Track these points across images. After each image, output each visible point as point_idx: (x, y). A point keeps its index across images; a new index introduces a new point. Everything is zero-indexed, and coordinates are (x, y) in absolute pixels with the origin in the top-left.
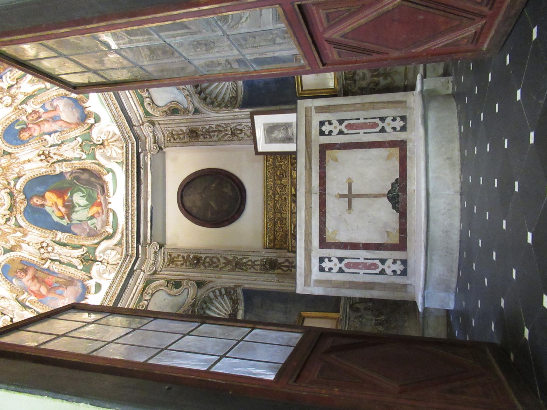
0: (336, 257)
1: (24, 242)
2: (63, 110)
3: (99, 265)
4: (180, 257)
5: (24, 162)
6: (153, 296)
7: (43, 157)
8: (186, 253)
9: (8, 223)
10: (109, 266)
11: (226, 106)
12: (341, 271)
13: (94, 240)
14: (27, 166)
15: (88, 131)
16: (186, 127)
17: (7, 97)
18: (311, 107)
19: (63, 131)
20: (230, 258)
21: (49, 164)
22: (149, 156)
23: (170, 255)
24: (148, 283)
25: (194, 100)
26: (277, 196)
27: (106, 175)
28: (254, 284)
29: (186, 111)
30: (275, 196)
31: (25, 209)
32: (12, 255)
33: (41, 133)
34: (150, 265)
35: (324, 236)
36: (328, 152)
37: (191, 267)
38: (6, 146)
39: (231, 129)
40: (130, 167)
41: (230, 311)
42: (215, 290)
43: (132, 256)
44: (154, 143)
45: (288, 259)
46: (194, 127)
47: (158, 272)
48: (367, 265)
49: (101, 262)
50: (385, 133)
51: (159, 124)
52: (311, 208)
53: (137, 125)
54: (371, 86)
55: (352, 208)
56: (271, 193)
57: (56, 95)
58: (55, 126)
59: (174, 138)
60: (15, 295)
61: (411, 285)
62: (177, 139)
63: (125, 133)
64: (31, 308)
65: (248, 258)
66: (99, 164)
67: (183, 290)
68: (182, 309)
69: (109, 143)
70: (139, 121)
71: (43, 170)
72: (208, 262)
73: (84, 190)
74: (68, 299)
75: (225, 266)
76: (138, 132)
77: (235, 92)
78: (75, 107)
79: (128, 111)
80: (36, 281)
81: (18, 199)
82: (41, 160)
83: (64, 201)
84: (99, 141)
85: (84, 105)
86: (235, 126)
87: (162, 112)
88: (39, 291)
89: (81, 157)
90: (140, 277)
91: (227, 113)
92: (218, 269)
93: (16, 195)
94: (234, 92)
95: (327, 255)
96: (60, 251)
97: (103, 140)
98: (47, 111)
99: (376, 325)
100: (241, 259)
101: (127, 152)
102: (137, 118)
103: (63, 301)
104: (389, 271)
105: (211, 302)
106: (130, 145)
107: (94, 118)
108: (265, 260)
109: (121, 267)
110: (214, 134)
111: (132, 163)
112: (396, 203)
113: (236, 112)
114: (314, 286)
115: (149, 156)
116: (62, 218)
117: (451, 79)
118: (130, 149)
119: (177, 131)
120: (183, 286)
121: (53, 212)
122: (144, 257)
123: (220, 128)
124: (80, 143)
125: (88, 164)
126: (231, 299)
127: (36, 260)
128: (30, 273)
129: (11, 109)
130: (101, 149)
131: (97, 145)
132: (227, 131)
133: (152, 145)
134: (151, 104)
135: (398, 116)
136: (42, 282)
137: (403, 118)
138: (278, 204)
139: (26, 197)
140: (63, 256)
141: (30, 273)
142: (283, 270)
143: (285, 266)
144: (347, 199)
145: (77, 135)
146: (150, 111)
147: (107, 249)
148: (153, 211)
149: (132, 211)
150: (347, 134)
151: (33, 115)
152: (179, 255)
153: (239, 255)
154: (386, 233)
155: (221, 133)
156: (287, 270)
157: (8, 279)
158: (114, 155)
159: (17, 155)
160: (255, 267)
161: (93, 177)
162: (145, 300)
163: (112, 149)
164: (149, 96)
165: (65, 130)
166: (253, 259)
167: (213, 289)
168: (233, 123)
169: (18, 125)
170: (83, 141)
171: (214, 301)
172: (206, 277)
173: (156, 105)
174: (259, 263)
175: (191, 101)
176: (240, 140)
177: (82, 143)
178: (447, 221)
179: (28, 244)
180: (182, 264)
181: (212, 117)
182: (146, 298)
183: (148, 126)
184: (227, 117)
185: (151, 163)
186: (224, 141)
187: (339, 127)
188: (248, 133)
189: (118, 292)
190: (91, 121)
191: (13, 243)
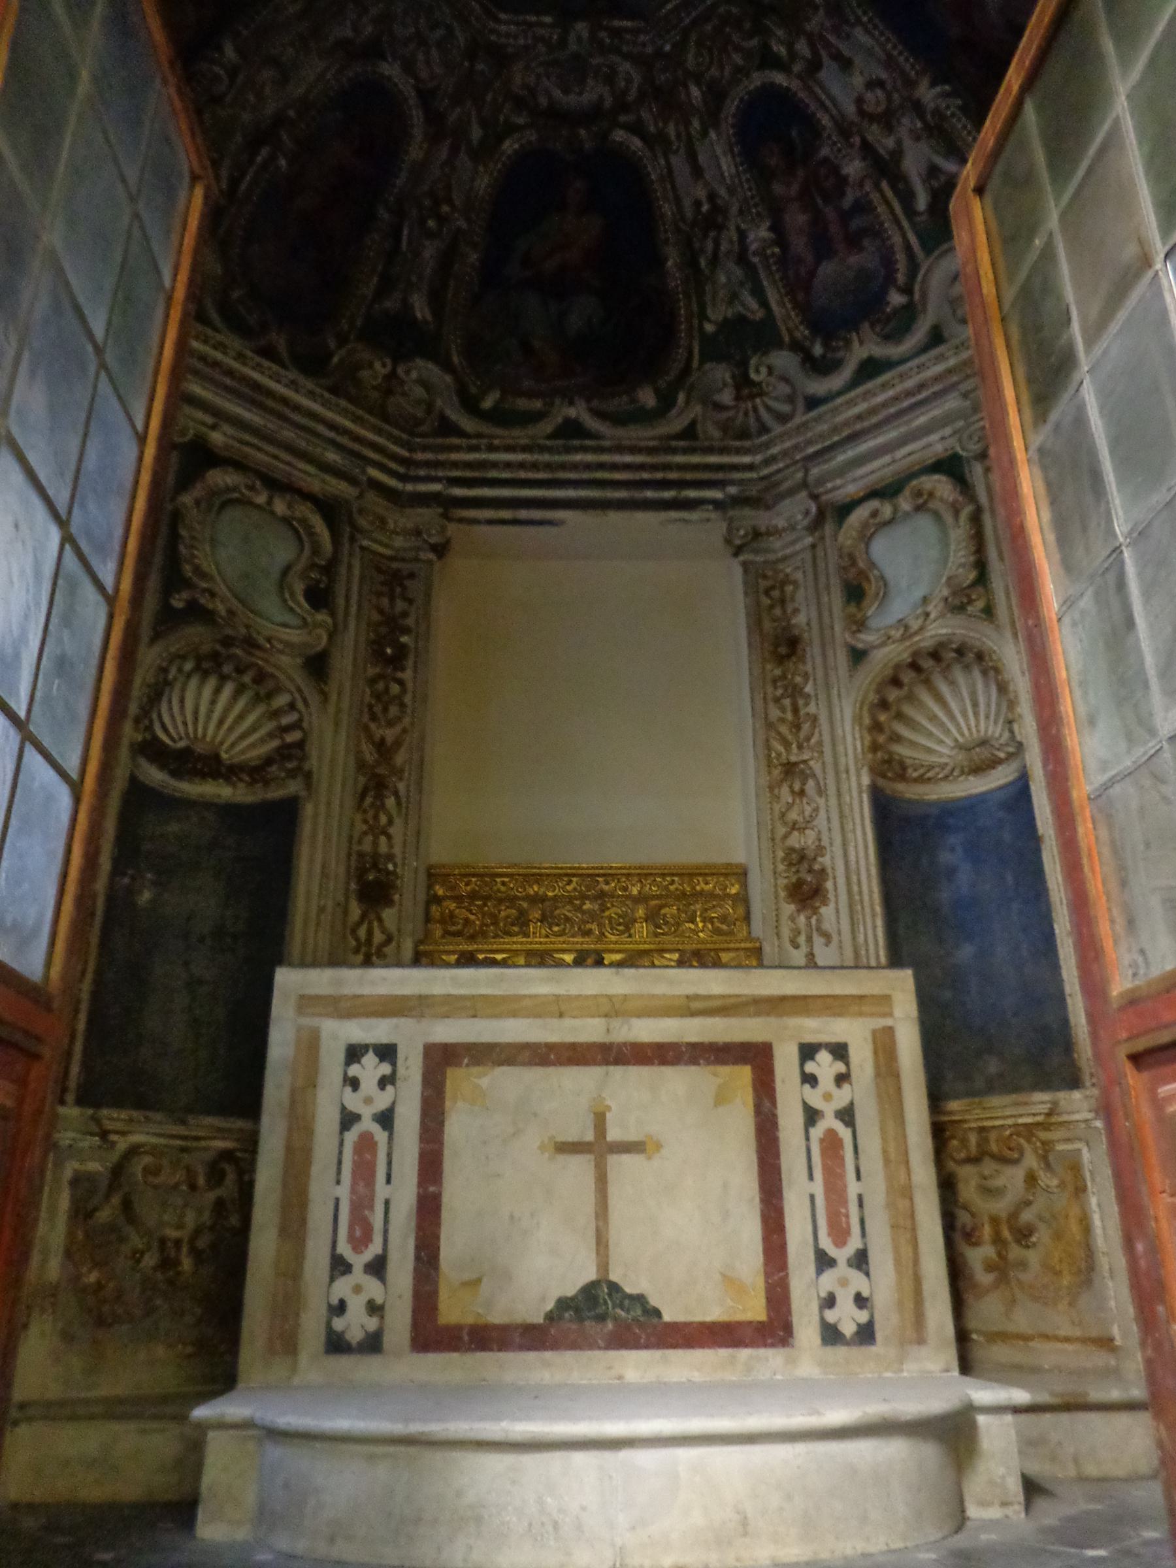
0: (394, 1103)
1: (454, 150)
5: (692, 156)
11: (875, 747)
12: (348, 1119)
15: (787, 339)
16: (808, 624)
18: (890, 1014)
20: (399, 759)
23: (412, 576)
25: (893, 646)
26: (597, 907)
28: (314, 835)
30: (595, 898)
35: (466, 1061)
36: (745, 1073)
39: (805, 762)
42: (300, 712)
45: (394, 944)
48: (367, 1212)
50: (812, 1268)
51: (813, 546)
52: (561, 1015)
54: (963, 1218)
55: (562, 1158)
56: (606, 888)
58: (799, 244)
59: (773, 588)
61: (294, 1369)
62: (771, 598)
68: (240, 605)
71: (668, 209)
72: (387, 690)
77: (922, 775)
82: (698, 204)
84: (757, 371)
86: (814, 776)
91: (855, 749)
94: (921, 771)
95: (401, 1071)
97: (760, 384)
98: (845, 217)
99: (163, 1242)
100: (396, 794)
104: (342, 1288)
105: (257, 699)
106: (746, 459)
108: (390, 867)
110: (789, 708)
112: (577, 1310)
113: (858, 776)
114: (299, 1029)
117: (1016, 1512)
119: (793, 599)
120: (313, 611)
123: (806, 727)
126: (268, 761)
132: (800, 747)
135: (872, 1316)
137: (866, 1334)
138: (569, 911)
142: (359, 924)
143: (370, 933)
144: (589, 1137)
150: (808, 1139)
152: (410, 601)
153: (408, 786)
154: (474, 1276)
156: (357, 939)
160: (370, 838)
166: (396, 830)
167: (300, 704)
173: (872, 535)
174: (383, 848)
175: (889, 638)
176: (771, 788)
178: (514, 1519)
180: (381, 611)
186: (767, 741)
187: (828, 1110)
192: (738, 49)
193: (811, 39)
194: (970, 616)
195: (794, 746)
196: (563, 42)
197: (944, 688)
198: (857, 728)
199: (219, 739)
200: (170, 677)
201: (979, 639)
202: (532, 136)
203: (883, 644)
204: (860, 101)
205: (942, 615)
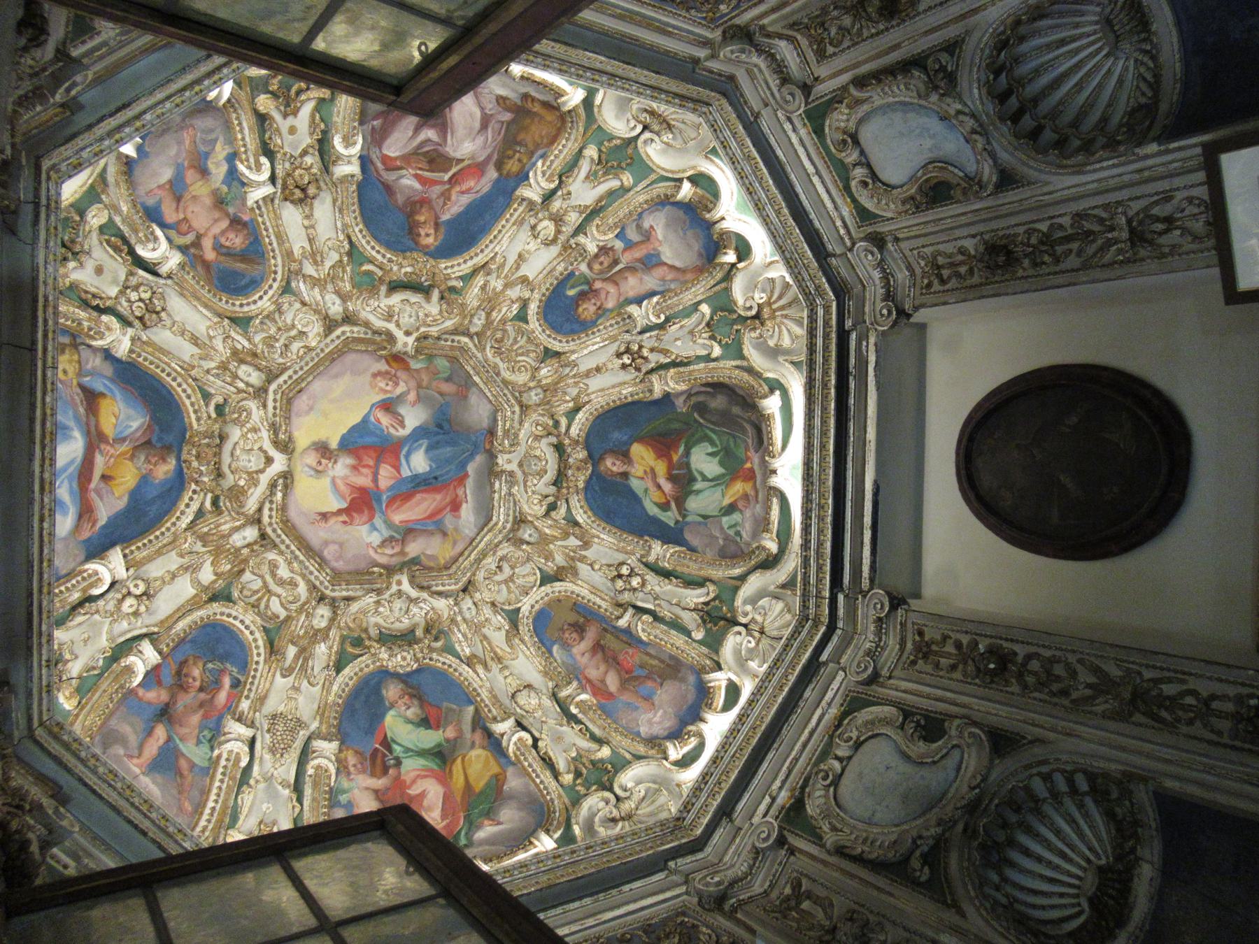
1: (582, 559)
2: (665, 237)
3: (740, 633)
4: (950, 642)
5: (588, 374)
6: (862, 750)
7: (626, 360)
8: (967, 632)
9: (553, 514)
10: (765, 642)
11: (1112, 144)
13: (733, 567)
14: (595, 383)
15: (723, 285)
16: (974, 236)
17: (546, 223)
20: (1115, 672)
21: (641, 375)
22: (872, 340)
23: (921, 633)
24: (853, 705)
27: (765, 397)
29: (973, 184)
31: (588, 482)
32: (557, 589)
33: (622, 299)
34: (861, 653)
37: (977, 681)
38: (549, 336)
39: (1129, 222)
40: (818, 374)
41: (1107, 858)
42: (1053, 771)
43: (816, 623)
44: (884, 300)
46: (1001, 233)
49: (745, 626)
53: (838, 252)
57: (646, 202)
59: (940, 277)
60: (550, 684)
62: (950, 278)
63: (807, 277)
64: (579, 722)
65: (1183, 682)
66: (750, 370)
67: (945, 751)
68: (935, 810)
69: (775, 311)
70: (842, 238)
72: (1035, 674)
73: (714, 436)
74: (660, 713)
75: (1093, 698)
76: (844, 272)
77: (1150, 85)
78: (691, 227)
79: (812, 216)
80: (599, 655)
81: (571, 460)
82: (624, 366)
83: (671, 466)
84: (751, 308)
85: (708, 216)
86: (1146, 209)
87: (904, 203)
88: (603, 681)
90: (835, 685)
91: (1114, 166)
92: (1066, 702)
93: (569, 450)
94: (1143, 86)
96: (657, 589)
98: (630, 246)
100: (1156, 681)
101: (812, 333)
103: (650, 715)
105: (1038, 812)
106: (820, 312)
107: (737, 250)
111: (826, 360)
113: (1147, 157)
115: (872, 340)
116: (665, 507)
118: (820, 322)
121: (646, 490)
122: (850, 629)
123: (1087, 225)
124: (708, 317)
125: (727, 370)
126: (1110, 815)
127: (604, 605)
128: (591, 634)
129: (555, 250)
130: (754, 329)
132: (1112, 229)
133: (879, 305)
134: (870, 181)
136: (612, 660)
139: (590, 456)
140: (663, 603)
141: (591, 634)
145: (699, 298)
146: (869, 205)
147: (761, 594)
148: (880, 498)
149: (822, 495)
151: (602, 259)
153: (1147, 666)
155: (1093, 241)
157: (543, 644)
158: (786, 342)
159: (573, 357)
160: (1213, 720)
161: (737, 404)
162: (837, 758)
164: (864, 160)
165: (673, 286)
166: (1205, 688)
167: (1044, 769)
168: (1137, 198)
169: (573, 287)
170: (713, 313)
171: (1048, 809)
172: (1025, 722)
173: (884, 184)
174: (1229, 707)
176: (1164, 256)
177: (712, 318)
179: (591, 565)
180: (953, 668)
181: (1057, 191)
182: (840, 753)
184: (1112, 182)
185: (877, 357)
186: (1103, 266)
188: (1199, 226)
189: (768, 720)
190: (730, 257)
191: (560, 560)
192: (516, 341)
193: (507, 286)
194: (958, 65)
195: (1110, 236)
196: (511, 474)
197: (1044, 80)
198: (1088, 168)
199: (1083, 864)
200: (1004, 901)
201: (982, 50)
202: (576, 502)
203: (993, 155)
204: (548, 243)
205: (959, 97)
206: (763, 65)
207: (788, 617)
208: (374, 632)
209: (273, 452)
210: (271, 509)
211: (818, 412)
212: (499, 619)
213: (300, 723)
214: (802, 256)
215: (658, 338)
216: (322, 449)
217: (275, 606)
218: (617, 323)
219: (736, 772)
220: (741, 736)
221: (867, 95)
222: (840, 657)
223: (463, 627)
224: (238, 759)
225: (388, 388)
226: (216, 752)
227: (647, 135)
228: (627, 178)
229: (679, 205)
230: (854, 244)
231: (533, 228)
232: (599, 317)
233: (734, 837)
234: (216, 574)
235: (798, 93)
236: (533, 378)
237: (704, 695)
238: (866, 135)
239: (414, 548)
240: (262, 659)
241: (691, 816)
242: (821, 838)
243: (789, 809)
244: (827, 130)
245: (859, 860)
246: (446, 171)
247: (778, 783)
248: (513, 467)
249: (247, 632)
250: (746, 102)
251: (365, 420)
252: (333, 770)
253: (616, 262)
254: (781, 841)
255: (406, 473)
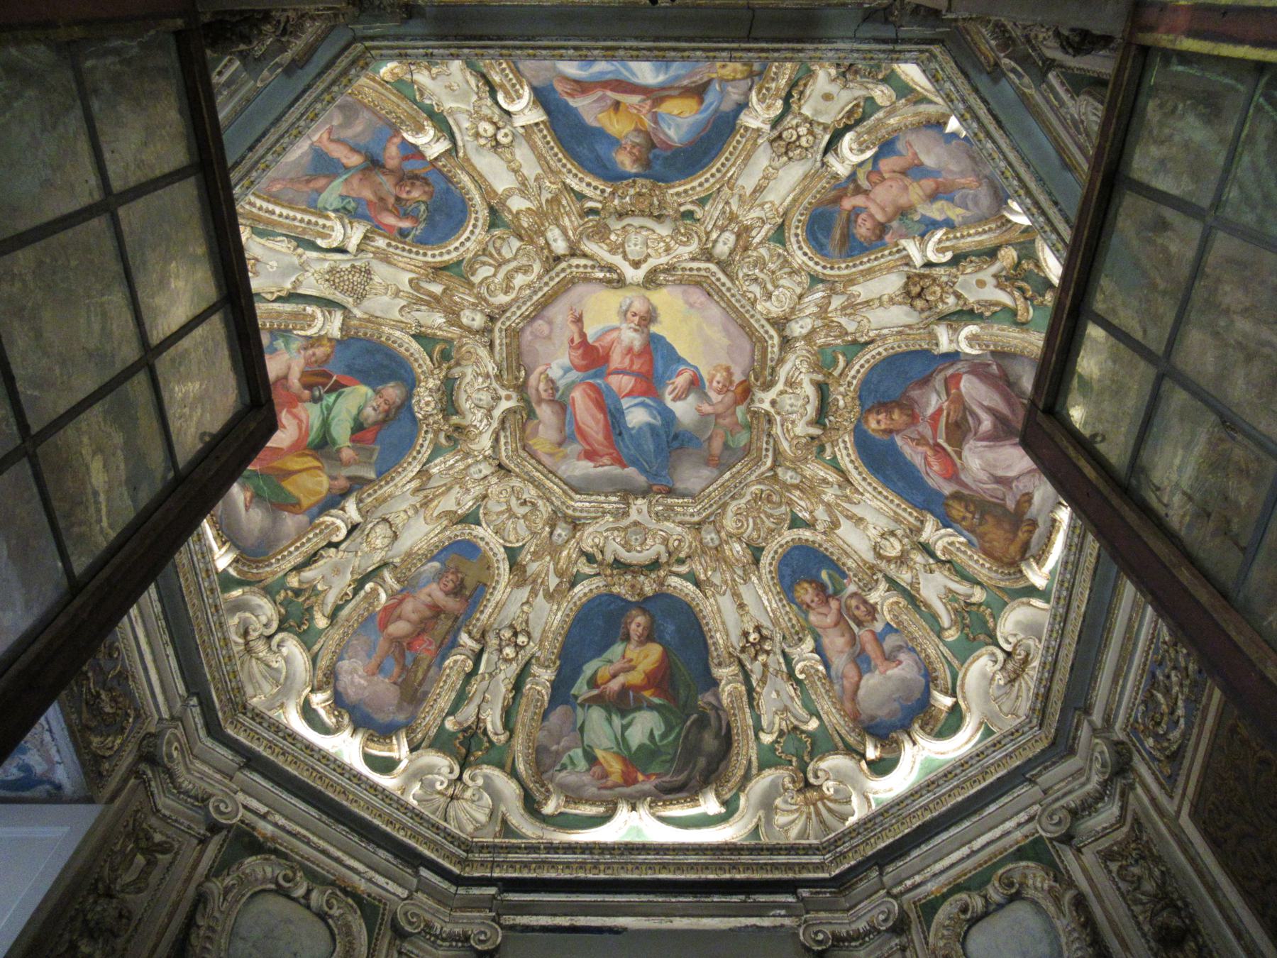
1: (534, 593)
2: (890, 678)
3: (451, 772)
5: (736, 595)
6: (316, 919)
7: (753, 637)
9: (583, 559)
10: (442, 801)
13: (526, 762)
14: (726, 603)
15: (840, 744)
17: (898, 547)
19: (831, 682)
21: (737, 653)
22: (787, 922)
24: (369, 908)
27: (718, 796)
31: (618, 597)
32: (501, 565)
33: (819, 631)
34: (428, 917)
38: (776, 552)
40: (746, 859)
43: (463, 862)
44: (833, 934)
47: (398, 942)
49: (460, 778)
53: (885, 879)
57: (928, 656)
58: (840, 662)
60: (397, 560)
63: (855, 842)
64: (356, 592)
66: (747, 778)
69: (815, 805)
70: (900, 883)
73: (671, 738)
76: (862, 886)
79: (924, 848)
80: (428, 613)
81: (642, 578)
82: (746, 634)
83: (637, 689)
84: (817, 777)
85: (916, 726)
88: (399, 617)
89: (763, 730)
90: (392, 886)
93: (653, 576)
96: (502, 676)
98: (878, 639)
101: (792, 849)
102: (908, 878)
103: (361, 672)
106: (816, 859)
107: (881, 759)
109: (433, 825)
111: (762, 867)
115: (787, 922)
116: (593, 683)
118: (804, 859)
121: (610, 662)
122: (456, 903)
124: (804, 727)
125: (746, 751)
127: (484, 617)
128: (451, 604)
129: (869, 557)
130: (793, 782)
131: (805, 773)
133: (828, 929)
134: (968, 916)
136: (422, 628)
139: (648, 599)
140: (486, 683)
141: (451, 604)
145: (824, 717)
146: (941, 915)
148: (607, 935)
149: (608, 866)
151: (863, 608)
157: (441, 551)
158: (780, 819)
159: (754, 579)
161: (709, 764)
162: (309, 892)
163: (796, 815)
164: (992, 908)
165: (836, 687)
169: (830, 576)
173: (966, 933)
177: (803, 732)
179: (527, 602)
182: (314, 895)
183: (889, 912)
185: (768, 928)
190: (872, 753)
191: (533, 567)
192: (769, 516)
193: (828, 505)
196: (626, 514)
202: (597, 583)
204: (876, 549)
206: (1089, 787)
207: (470, 828)
208: (456, 372)
209: (645, 268)
210: (585, 266)
211: (703, 859)
212: (468, 504)
213: (360, 298)
214: (879, 837)
215: (777, 672)
216: (649, 317)
217: (484, 272)
218: (793, 626)
219: (296, 773)
220: (335, 777)
221: (1066, 908)
222: (424, 892)
223: (461, 466)
224: (325, 236)
225: (715, 384)
226: (332, 215)
227: (1001, 656)
228: (952, 635)
229: (927, 694)
230: (895, 897)
231: (892, 533)
232: (799, 606)
233: (219, 771)
234: (518, 213)
235: (1062, 830)
236: (730, 535)
237: (383, 732)
238: (1021, 911)
239: (545, 412)
240: (429, 259)
241: (247, 721)
242: (217, 875)
243: (251, 836)
244: (1023, 864)
245: (190, 923)
246: (948, 441)
247: (282, 821)
248: (634, 516)
249: (457, 244)
250: (1046, 768)
251: (680, 360)
252: (309, 332)
253: (860, 624)
254: (214, 828)
255: (625, 403)
